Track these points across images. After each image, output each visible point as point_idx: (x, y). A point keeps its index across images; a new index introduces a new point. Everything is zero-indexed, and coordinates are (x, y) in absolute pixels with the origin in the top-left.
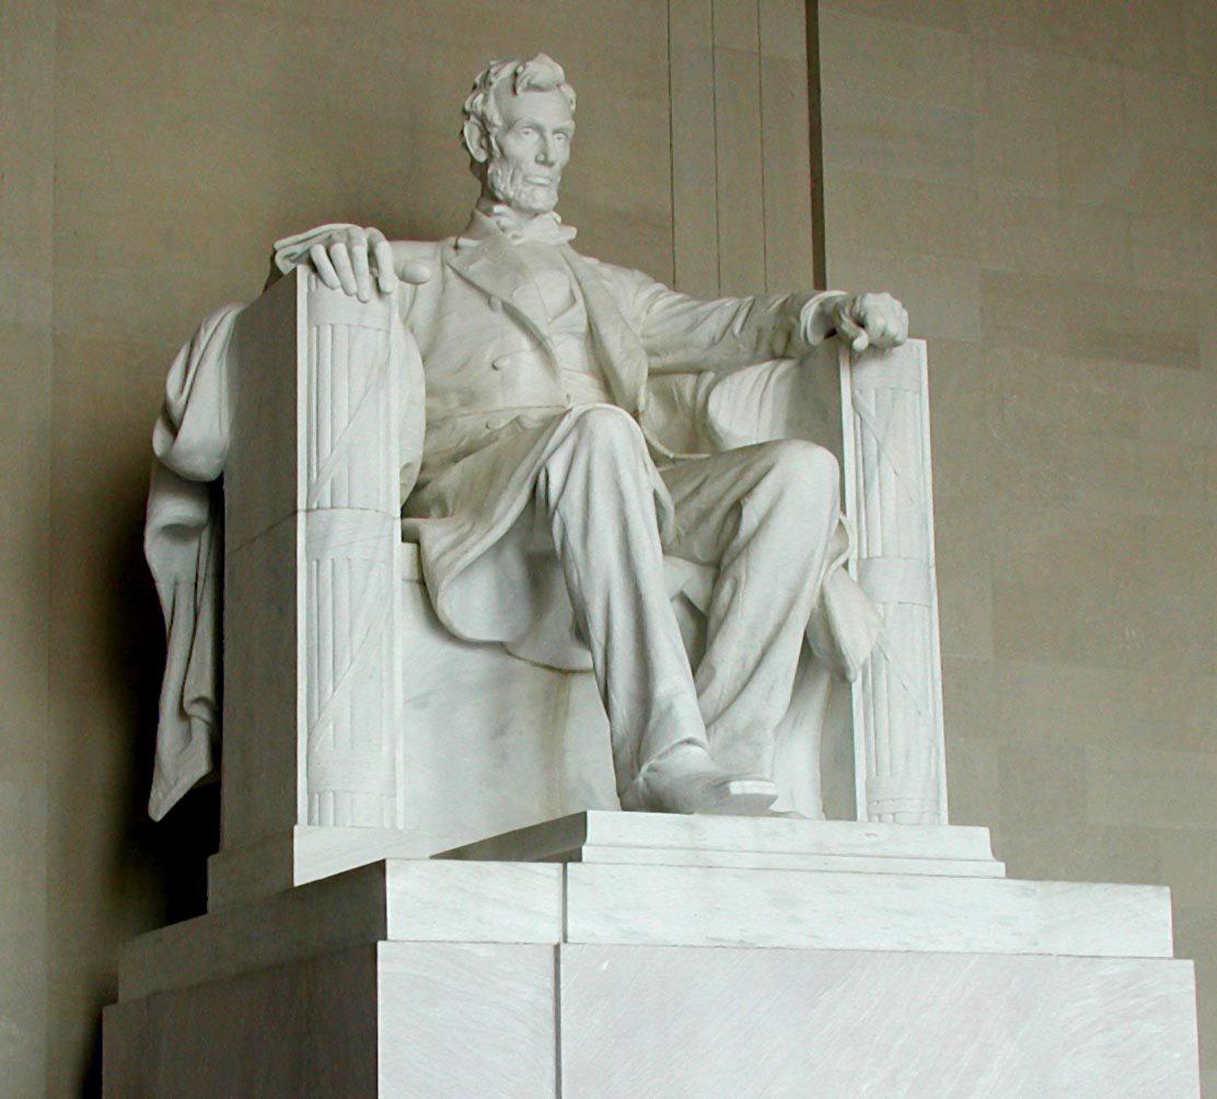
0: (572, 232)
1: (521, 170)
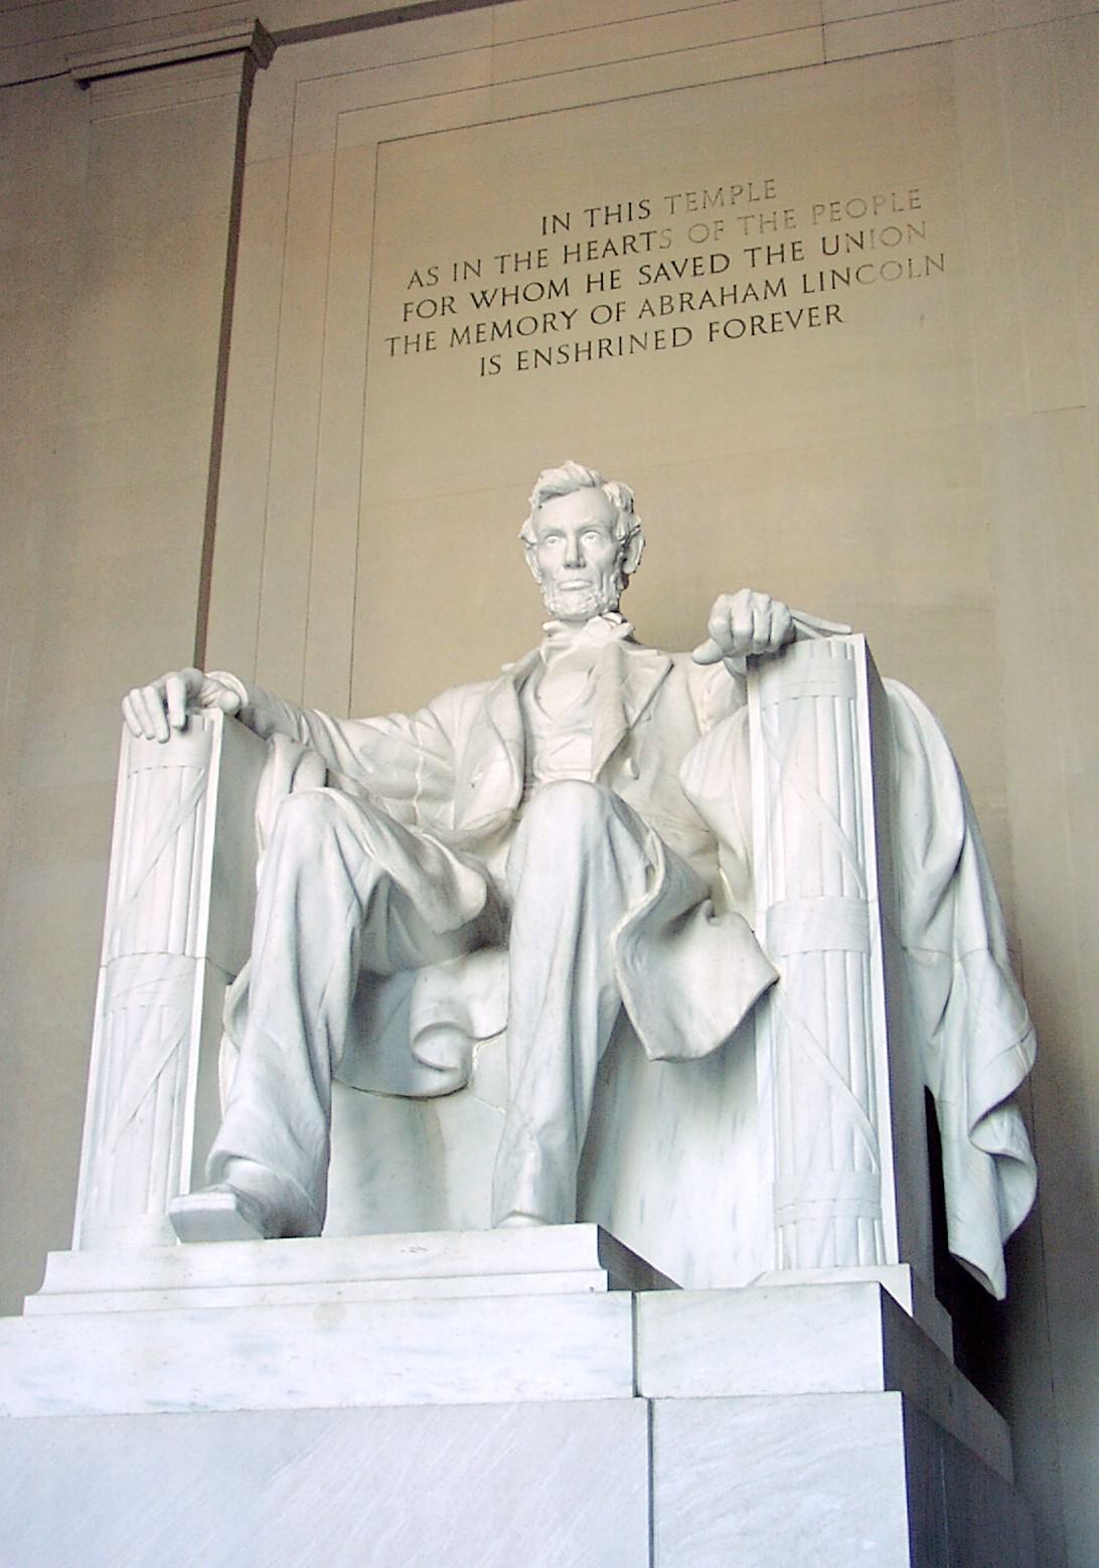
0: (624, 630)
1: (554, 580)
